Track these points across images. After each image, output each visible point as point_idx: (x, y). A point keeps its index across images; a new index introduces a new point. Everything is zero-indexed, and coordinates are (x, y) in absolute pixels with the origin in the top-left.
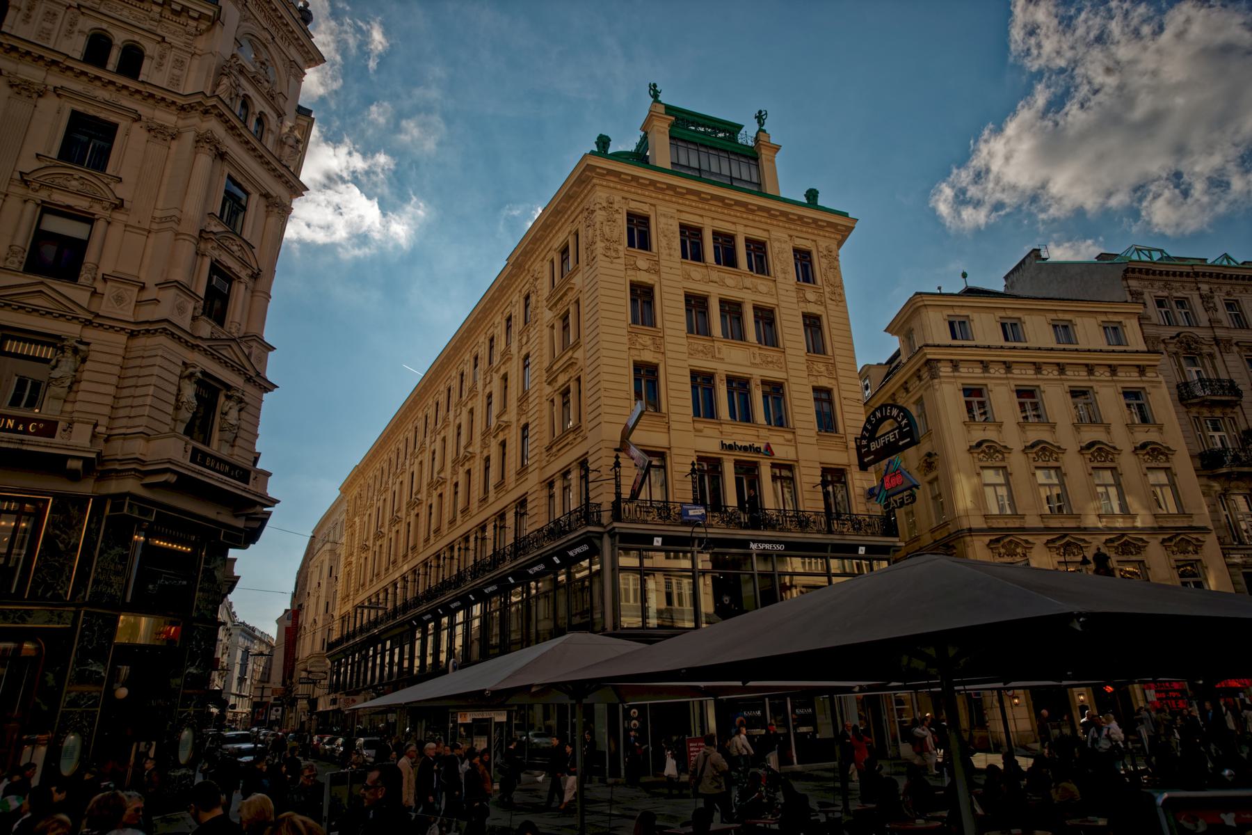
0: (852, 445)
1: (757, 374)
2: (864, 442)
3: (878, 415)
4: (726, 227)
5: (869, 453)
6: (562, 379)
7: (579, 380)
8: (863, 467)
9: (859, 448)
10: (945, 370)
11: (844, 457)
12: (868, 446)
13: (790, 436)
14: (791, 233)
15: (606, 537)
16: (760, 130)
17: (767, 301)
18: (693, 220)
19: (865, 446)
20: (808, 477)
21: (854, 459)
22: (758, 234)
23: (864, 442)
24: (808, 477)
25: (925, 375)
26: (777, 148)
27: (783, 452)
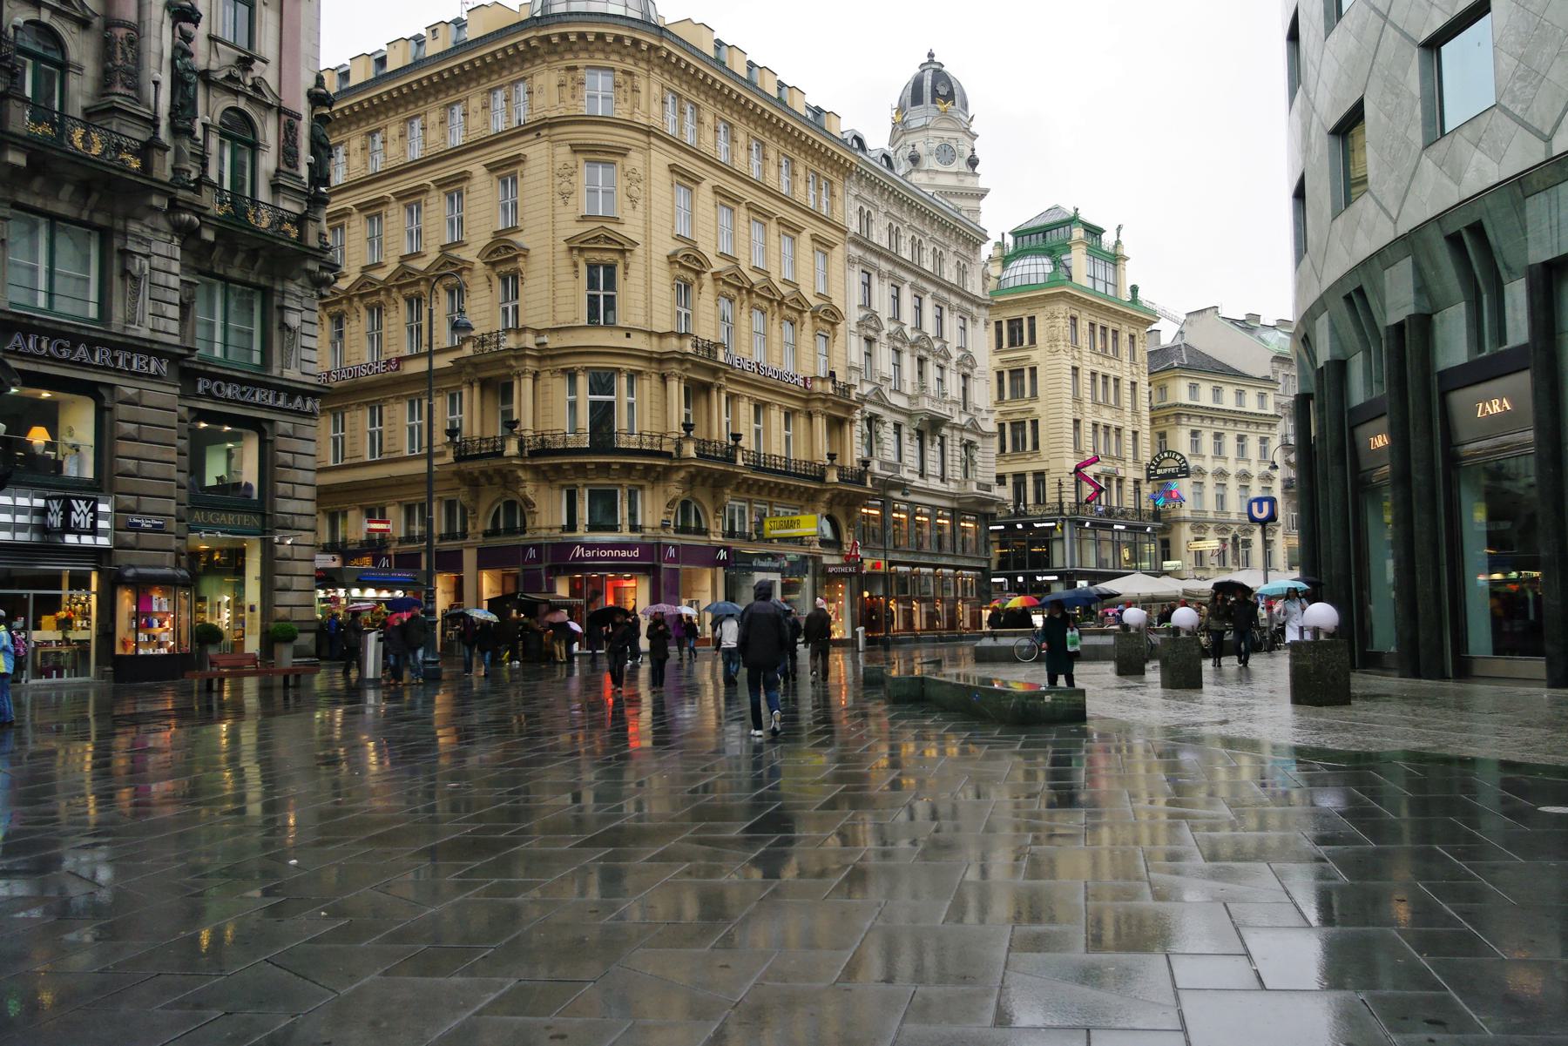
1: (1114, 424)
4: (1105, 323)
6: (1017, 416)
7: (1035, 423)
8: (1149, 480)
9: (1148, 470)
11: (1142, 475)
16: (1118, 242)
17: (1118, 374)
18: (1093, 319)
20: (1129, 487)
22: (1116, 326)
24: (1129, 487)
25: (1172, 420)
26: (1126, 259)
27: (1121, 473)
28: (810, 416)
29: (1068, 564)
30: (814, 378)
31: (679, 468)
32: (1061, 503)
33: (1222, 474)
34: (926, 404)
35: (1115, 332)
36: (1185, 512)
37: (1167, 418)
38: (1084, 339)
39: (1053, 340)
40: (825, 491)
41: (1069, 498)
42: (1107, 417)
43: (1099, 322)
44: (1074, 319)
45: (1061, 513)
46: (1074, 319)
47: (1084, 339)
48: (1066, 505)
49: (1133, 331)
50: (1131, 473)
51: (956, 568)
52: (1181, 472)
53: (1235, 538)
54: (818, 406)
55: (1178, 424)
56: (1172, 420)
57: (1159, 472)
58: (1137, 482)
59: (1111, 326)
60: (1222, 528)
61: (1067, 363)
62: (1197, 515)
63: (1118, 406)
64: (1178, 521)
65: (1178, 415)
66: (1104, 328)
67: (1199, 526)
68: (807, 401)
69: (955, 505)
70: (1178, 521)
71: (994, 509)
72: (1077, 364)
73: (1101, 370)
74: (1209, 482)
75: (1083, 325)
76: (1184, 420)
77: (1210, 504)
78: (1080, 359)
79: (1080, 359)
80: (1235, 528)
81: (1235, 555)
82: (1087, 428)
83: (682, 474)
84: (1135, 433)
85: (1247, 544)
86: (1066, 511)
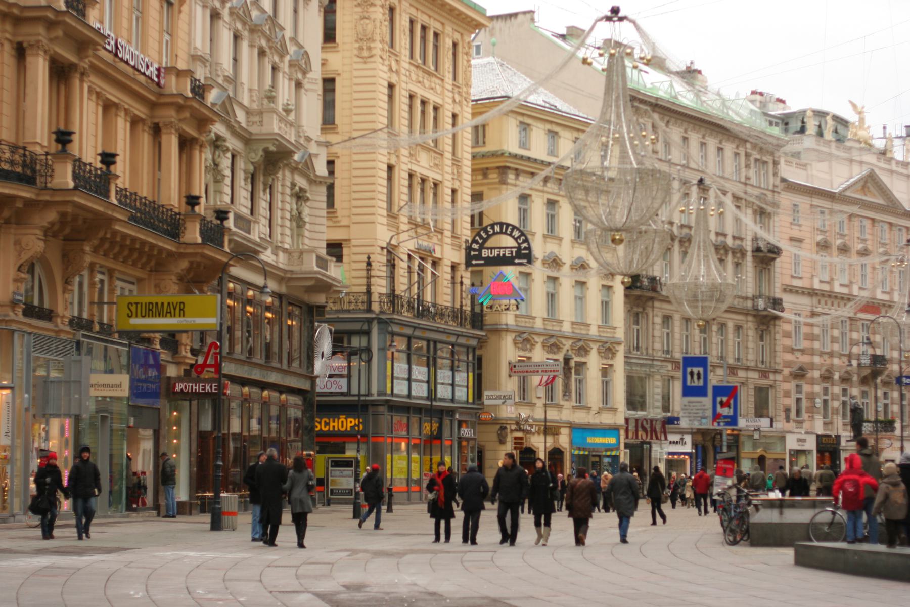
0: (464, 246)
1: (433, 175)
2: (475, 246)
3: (497, 228)
5: (479, 257)
8: (468, 264)
9: (469, 249)
10: (511, 177)
11: (459, 257)
12: (480, 251)
13: (440, 236)
14: (455, 27)
15: (375, 322)
17: (439, 101)
19: (475, 250)
20: (445, 273)
21: (463, 260)
22: (438, 26)
23: (475, 246)
24: (445, 273)
25: (494, 176)
28: (156, 131)
29: (374, 390)
30: (171, 70)
31: (47, 205)
32: (369, 293)
33: (554, 262)
34: (275, 126)
35: (436, 35)
36: (509, 319)
37: (485, 172)
38: (402, 41)
39: (364, 40)
40: (182, 256)
41: (380, 287)
42: (424, 166)
43: (422, 18)
44: (392, 10)
45: (369, 310)
46: (392, 10)
47: (402, 41)
48: (375, 297)
49: (457, 36)
50: (451, 254)
51: (263, 386)
52: (519, 255)
53: (567, 360)
54: (170, 114)
55: (503, 182)
56: (494, 176)
57: (485, 253)
58: (454, 267)
59: (434, 25)
60: (553, 346)
61: (383, 77)
62: (523, 322)
63: (435, 149)
64: (498, 331)
65: (503, 170)
66: (424, 28)
67: (525, 339)
68: (153, 106)
69: (283, 290)
70: (498, 331)
71: (321, 299)
72: (394, 79)
73: (420, 92)
74: (538, 271)
75: (402, 22)
76: (511, 177)
77: (538, 306)
78: (397, 72)
79: (397, 72)
80: (568, 344)
81: (567, 387)
82: (401, 178)
83: (52, 216)
84: (454, 191)
85: (581, 366)
86: (375, 307)
